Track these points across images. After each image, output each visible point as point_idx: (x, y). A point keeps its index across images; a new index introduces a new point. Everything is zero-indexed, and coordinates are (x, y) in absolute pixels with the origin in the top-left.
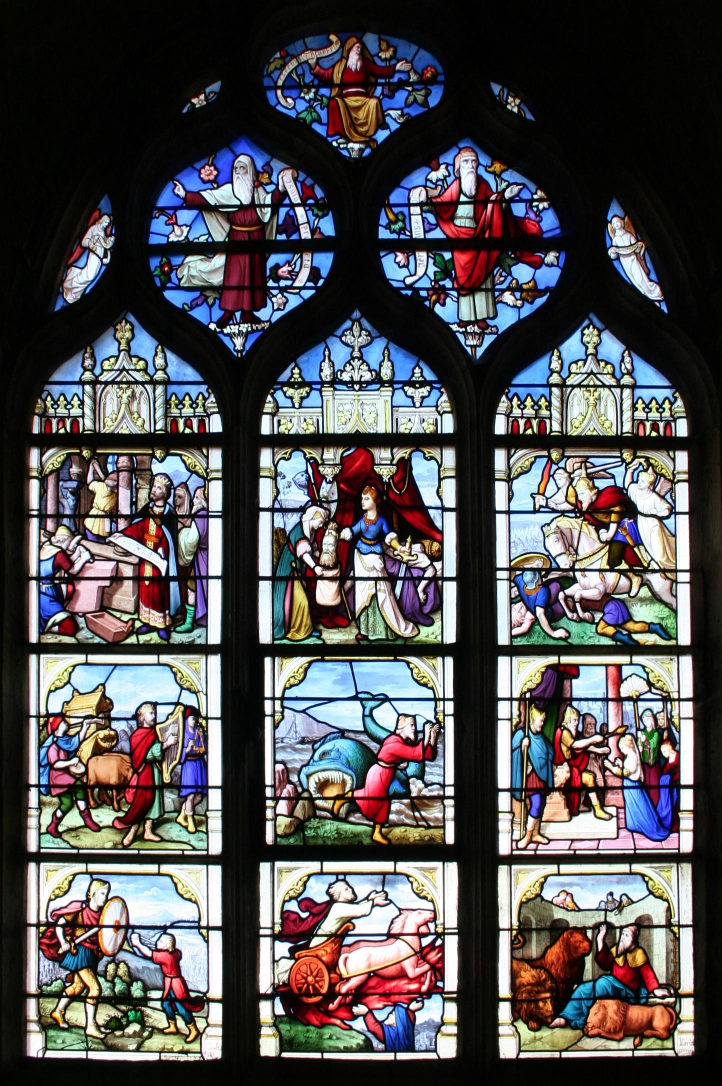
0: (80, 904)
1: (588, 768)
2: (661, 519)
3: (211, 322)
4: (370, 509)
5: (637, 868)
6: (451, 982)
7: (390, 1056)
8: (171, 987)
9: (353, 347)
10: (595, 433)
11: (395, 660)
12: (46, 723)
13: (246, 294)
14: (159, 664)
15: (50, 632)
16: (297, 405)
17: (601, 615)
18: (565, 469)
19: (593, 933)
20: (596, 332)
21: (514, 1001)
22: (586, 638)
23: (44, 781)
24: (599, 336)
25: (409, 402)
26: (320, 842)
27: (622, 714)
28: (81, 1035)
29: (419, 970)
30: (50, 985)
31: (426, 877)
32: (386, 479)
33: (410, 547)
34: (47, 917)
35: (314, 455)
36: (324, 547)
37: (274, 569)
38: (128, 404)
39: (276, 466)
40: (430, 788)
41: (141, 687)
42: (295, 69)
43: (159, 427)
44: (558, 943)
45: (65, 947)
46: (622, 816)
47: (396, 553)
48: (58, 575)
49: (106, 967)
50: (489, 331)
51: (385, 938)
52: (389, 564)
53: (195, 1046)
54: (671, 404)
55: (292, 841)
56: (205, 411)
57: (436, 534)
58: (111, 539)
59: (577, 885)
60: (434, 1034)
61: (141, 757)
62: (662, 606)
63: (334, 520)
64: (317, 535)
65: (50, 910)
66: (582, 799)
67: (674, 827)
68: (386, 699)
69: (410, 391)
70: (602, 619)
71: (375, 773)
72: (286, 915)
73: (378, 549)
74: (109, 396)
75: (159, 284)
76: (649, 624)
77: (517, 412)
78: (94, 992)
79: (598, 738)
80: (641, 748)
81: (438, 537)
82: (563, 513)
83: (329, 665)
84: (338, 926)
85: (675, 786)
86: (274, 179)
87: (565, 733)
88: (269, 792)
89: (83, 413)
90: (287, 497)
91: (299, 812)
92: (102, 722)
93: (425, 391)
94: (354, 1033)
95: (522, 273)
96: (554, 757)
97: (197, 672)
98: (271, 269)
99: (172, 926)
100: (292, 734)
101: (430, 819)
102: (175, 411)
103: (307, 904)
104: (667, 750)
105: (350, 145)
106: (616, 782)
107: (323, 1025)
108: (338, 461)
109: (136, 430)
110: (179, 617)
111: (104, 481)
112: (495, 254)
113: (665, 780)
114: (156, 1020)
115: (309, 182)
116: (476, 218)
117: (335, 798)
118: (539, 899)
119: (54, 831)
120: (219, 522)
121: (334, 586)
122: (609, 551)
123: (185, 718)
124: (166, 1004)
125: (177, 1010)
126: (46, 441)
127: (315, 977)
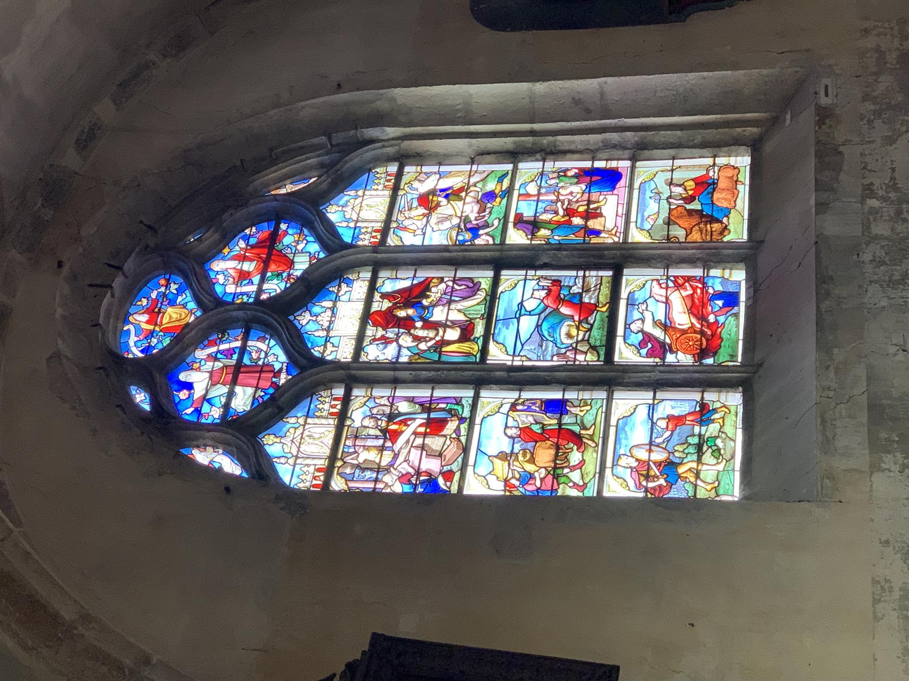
63: (409, 331)
68: (521, 304)
71: (565, 310)
79: (559, 204)
83: (497, 331)
92: (513, 457)
97: (489, 403)
121: (448, 330)
123: (518, 411)
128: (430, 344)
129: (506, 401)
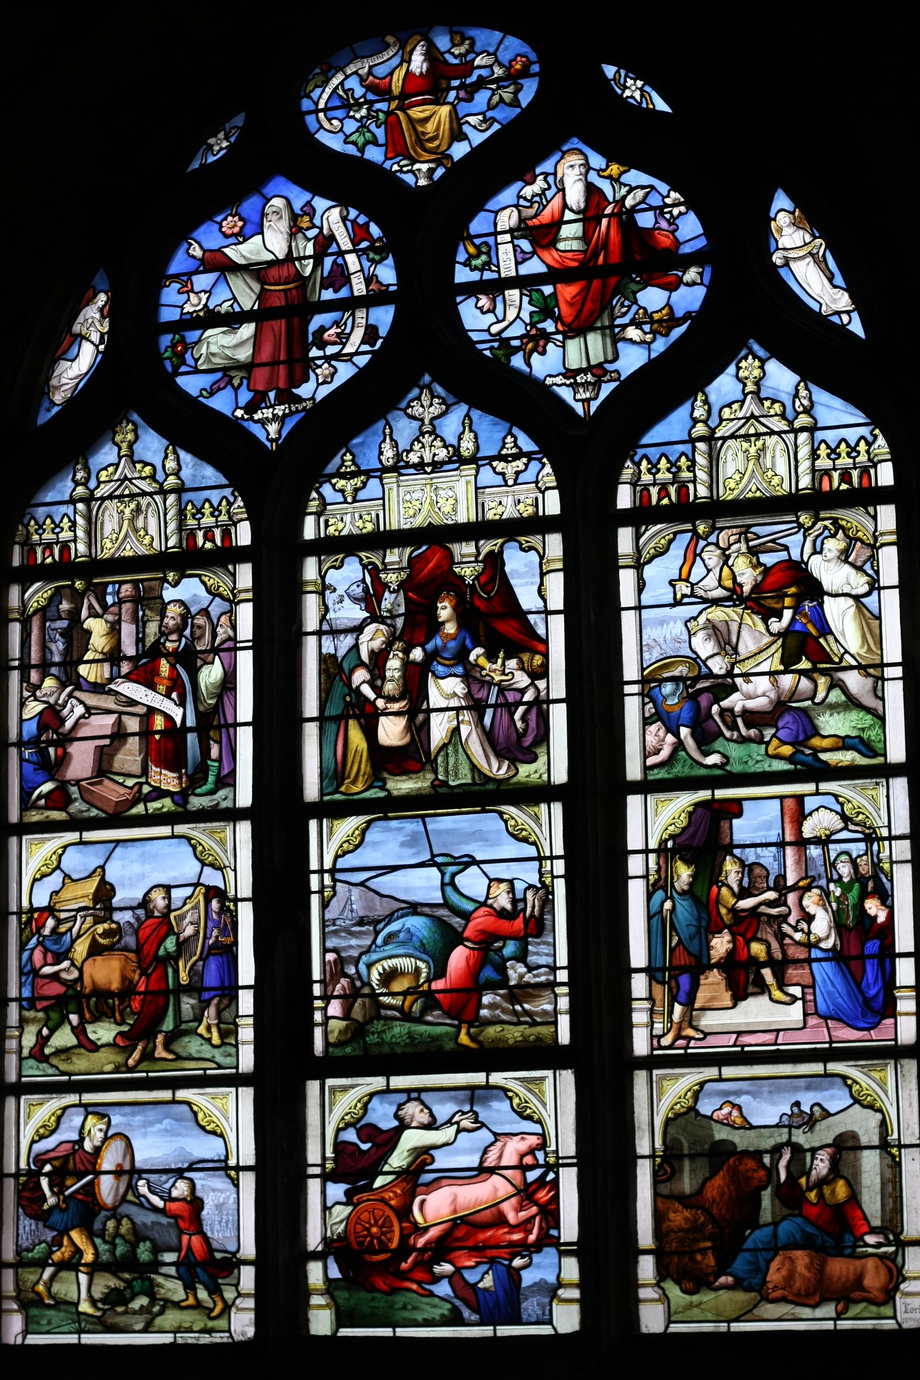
0: (71, 1145)
1: (759, 935)
2: (857, 598)
3: (237, 407)
4: (448, 621)
5: (835, 1067)
6: (569, 1227)
7: (486, 1331)
8: (189, 1247)
9: (422, 420)
10: (758, 494)
11: (484, 811)
12: (30, 920)
13: (282, 369)
14: (173, 837)
15: (35, 806)
16: (349, 499)
17: (773, 731)
18: (717, 545)
19: (772, 1159)
20: (757, 363)
21: (658, 1253)
22: (751, 763)
23: (26, 993)
24: (762, 367)
25: (499, 480)
26: (386, 1050)
27: (804, 861)
28: (72, 1313)
29: (523, 1215)
30: (32, 1251)
31: (530, 1090)
32: (469, 581)
33: (503, 664)
34: (28, 1164)
35: (374, 560)
36: (388, 674)
37: (323, 705)
38: (132, 520)
39: (323, 578)
40: (535, 972)
41: (151, 867)
42: (342, 83)
43: (170, 544)
44: (721, 1173)
45: (51, 1201)
46: (810, 997)
47: (484, 673)
48: (43, 738)
49: (105, 1224)
50: (608, 377)
51: (475, 1173)
52: (475, 688)
53: (221, 1323)
54: (869, 444)
55: (348, 1050)
56: (230, 518)
57: (541, 645)
58: (112, 686)
59: (748, 1093)
60: (547, 1300)
61: (152, 954)
62: (862, 714)
63: (400, 639)
64: (379, 659)
65: (32, 1155)
66: (752, 977)
67: (889, 1010)
69: (500, 466)
70: (774, 735)
71: (458, 957)
72: (341, 1147)
73: (459, 670)
74: (107, 513)
75: (169, 369)
76: (844, 738)
77: (646, 478)
78: (89, 1257)
79: (771, 895)
80: (834, 905)
81: (541, 647)
82: (716, 602)
83: (394, 824)
84: (410, 1159)
85: (888, 955)
86: (317, 221)
87: (724, 890)
88: (317, 990)
89: (75, 536)
90: (339, 614)
91: (357, 1011)
92: (102, 914)
93: (520, 464)
94: (437, 1300)
95: (652, 298)
96: (709, 923)
97: (222, 843)
98: (314, 334)
99: (190, 1169)
100: (347, 914)
101: (537, 1014)
102: (191, 522)
103: (369, 1132)
104: (873, 907)
105: (417, 166)
106: (801, 954)
107: (394, 1291)
108: (405, 564)
109: (143, 551)
110: (200, 775)
111: (101, 617)
112: (613, 280)
113: (872, 946)
114: (169, 1290)
115: (362, 220)
116: (586, 238)
117: (404, 994)
118: (693, 1114)
119: (38, 1054)
120: (249, 654)
121: (402, 722)
122: (783, 646)
123: (208, 902)
124: (182, 1269)
125: (197, 1277)
126: (30, 574)
127: (381, 1227)
128: (367, 690)
129: (231, 874)
